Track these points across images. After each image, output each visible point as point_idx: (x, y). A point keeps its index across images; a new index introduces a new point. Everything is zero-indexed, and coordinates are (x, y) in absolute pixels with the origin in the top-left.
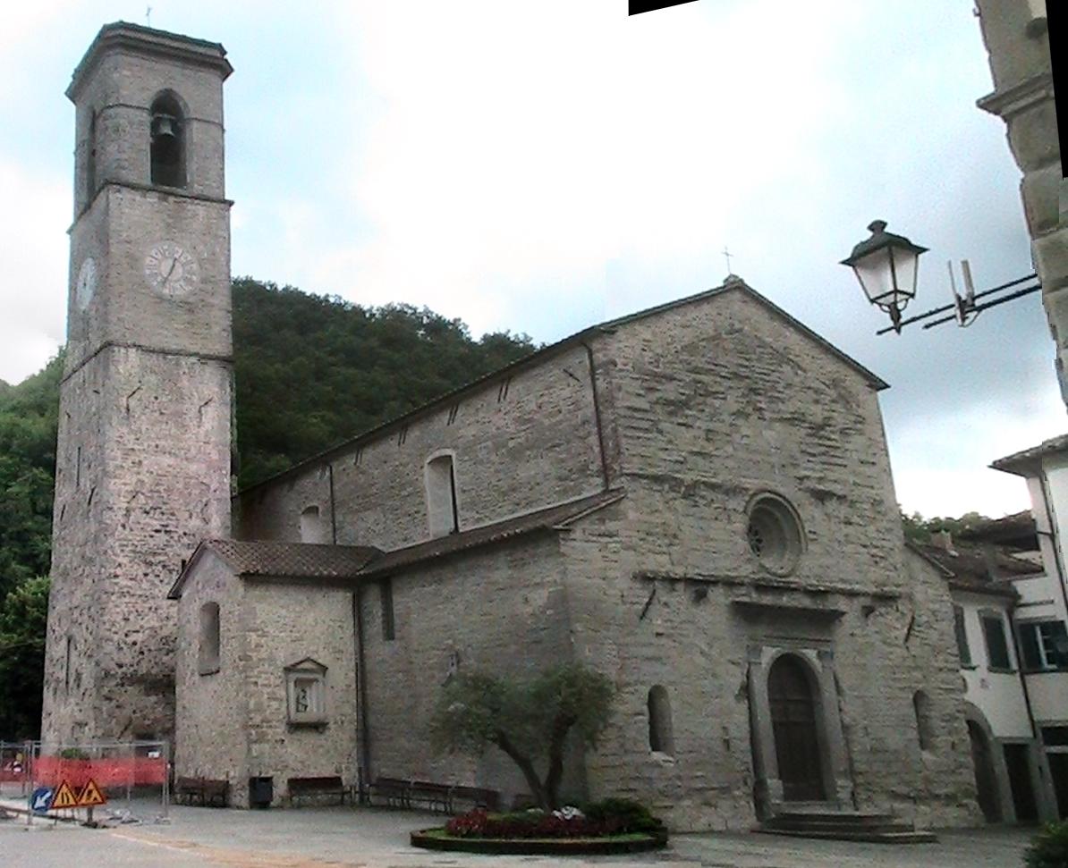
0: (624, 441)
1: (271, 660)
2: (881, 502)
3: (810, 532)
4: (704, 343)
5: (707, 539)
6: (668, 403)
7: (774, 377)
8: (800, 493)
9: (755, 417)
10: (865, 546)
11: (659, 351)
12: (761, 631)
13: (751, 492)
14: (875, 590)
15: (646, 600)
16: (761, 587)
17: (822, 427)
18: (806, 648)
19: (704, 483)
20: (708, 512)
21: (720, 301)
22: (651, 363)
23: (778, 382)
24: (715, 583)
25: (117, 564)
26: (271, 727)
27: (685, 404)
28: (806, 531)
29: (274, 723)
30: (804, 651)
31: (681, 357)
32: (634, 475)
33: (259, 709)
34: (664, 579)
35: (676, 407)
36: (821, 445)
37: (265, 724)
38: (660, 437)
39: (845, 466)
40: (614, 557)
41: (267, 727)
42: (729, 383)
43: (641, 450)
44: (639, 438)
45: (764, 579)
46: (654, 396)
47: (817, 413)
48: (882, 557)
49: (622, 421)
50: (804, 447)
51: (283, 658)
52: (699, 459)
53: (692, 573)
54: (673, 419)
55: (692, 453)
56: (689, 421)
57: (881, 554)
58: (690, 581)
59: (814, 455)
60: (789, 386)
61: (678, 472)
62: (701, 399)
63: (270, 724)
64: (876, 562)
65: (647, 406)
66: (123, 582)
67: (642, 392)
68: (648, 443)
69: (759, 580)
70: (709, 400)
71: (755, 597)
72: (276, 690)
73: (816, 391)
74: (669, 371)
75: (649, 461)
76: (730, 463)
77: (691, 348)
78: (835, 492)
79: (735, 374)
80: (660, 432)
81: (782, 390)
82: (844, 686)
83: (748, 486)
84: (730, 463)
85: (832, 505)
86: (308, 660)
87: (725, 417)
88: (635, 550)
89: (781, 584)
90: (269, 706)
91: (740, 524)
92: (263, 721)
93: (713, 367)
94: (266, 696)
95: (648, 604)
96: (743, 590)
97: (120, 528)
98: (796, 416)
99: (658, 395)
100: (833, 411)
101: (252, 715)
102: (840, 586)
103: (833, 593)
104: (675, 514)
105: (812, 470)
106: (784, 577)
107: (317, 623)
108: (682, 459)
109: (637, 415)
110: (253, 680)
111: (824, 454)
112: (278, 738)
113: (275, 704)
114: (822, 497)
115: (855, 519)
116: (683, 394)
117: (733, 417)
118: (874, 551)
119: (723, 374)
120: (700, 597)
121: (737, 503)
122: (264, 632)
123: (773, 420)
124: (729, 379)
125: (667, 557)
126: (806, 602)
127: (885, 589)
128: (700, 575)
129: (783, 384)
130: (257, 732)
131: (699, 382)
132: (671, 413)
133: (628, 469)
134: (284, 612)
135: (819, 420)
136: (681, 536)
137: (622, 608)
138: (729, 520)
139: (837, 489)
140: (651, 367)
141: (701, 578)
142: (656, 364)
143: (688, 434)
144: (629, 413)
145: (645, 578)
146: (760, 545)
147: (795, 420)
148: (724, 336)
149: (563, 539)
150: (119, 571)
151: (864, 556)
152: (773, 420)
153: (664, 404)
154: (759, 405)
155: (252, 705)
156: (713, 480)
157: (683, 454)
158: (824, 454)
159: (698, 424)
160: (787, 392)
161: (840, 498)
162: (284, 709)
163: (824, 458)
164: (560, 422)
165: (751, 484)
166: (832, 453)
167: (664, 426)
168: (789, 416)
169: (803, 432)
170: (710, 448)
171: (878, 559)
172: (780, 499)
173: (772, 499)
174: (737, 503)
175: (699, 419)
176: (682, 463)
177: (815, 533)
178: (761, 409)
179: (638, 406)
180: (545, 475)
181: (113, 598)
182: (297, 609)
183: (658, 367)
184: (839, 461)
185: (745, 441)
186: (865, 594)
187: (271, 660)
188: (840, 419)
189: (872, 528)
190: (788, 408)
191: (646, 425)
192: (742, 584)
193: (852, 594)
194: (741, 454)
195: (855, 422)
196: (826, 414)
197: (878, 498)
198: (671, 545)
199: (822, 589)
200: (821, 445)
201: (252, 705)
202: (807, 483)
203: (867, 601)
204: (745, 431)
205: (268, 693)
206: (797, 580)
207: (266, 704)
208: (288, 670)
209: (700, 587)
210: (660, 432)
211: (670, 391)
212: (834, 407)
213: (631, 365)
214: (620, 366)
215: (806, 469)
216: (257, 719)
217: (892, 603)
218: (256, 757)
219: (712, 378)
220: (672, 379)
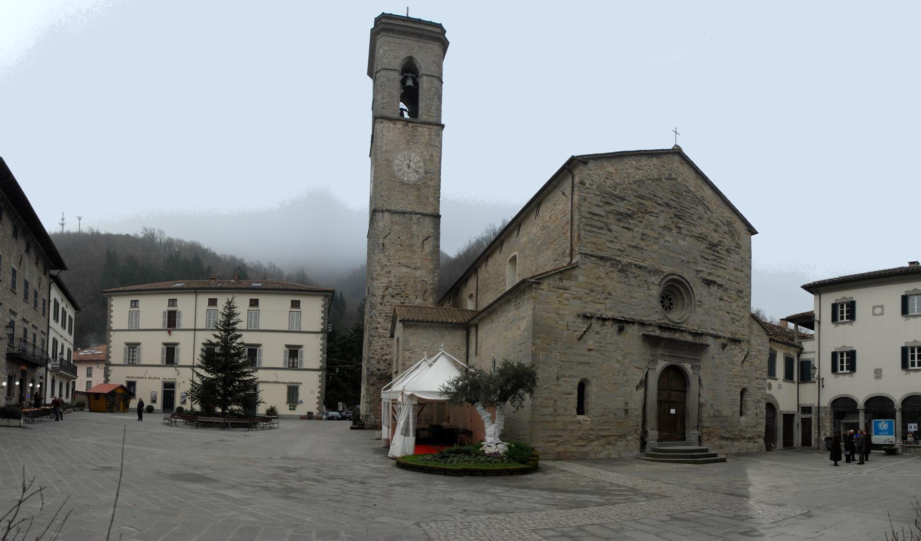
0: (583, 232)
2: (741, 292)
3: (698, 301)
4: (649, 182)
5: (631, 297)
6: (619, 214)
7: (692, 211)
8: (696, 279)
9: (675, 231)
10: (729, 313)
11: (618, 181)
12: (660, 352)
13: (665, 274)
14: (730, 336)
15: (585, 329)
16: (661, 328)
17: (716, 246)
18: (684, 362)
19: (636, 265)
20: (633, 282)
21: (664, 158)
22: (611, 187)
23: (694, 215)
24: (633, 322)
27: (630, 216)
28: (696, 299)
30: (683, 364)
31: (632, 187)
32: (586, 254)
34: (598, 318)
35: (622, 217)
36: (712, 255)
38: (609, 233)
39: (726, 269)
40: (566, 302)
42: (662, 209)
43: (594, 240)
44: (594, 232)
45: (664, 323)
46: (609, 208)
47: (715, 237)
48: (737, 320)
49: (584, 220)
50: (702, 254)
52: (634, 251)
53: (618, 316)
54: (622, 224)
55: (630, 246)
56: (631, 226)
57: (737, 318)
58: (615, 320)
59: (708, 260)
60: (701, 218)
61: (619, 256)
62: (640, 215)
64: (734, 322)
65: (603, 214)
67: (601, 204)
68: (599, 236)
69: (662, 324)
70: (647, 216)
71: (658, 333)
73: (717, 225)
74: (622, 195)
75: (599, 247)
76: (654, 256)
77: (640, 182)
78: (717, 282)
79: (667, 204)
81: (696, 219)
82: (703, 383)
83: (665, 270)
84: (654, 256)
85: (714, 288)
87: (656, 228)
88: (581, 300)
89: (675, 327)
91: (656, 291)
93: (652, 197)
95: (585, 332)
96: (651, 329)
98: (702, 236)
99: (613, 208)
100: (724, 238)
102: (711, 332)
103: (706, 335)
104: (613, 281)
105: (705, 268)
106: (678, 323)
108: (622, 249)
111: (714, 260)
114: (709, 283)
115: (725, 298)
116: (630, 210)
117: (661, 229)
118: (733, 316)
119: (658, 202)
120: (621, 330)
121: (655, 279)
123: (687, 235)
124: (663, 206)
125: (603, 306)
126: (689, 338)
127: (736, 336)
128: (624, 318)
129: (696, 216)
131: (642, 204)
132: (619, 220)
133: (584, 250)
135: (716, 241)
136: (614, 294)
137: (565, 333)
138: (649, 289)
139: (718, 280)
140: (609, 190)
141: (623, 319)
142: (613, 188)
143: (628, 234)
144: (590, 216)
145: (586, 317)
147: (700, 238)
148: (664, 180)
149: (535, 288)
151: (727, 318)
152: (687, 235)
154: (679, 225)
156: (642, 264)
157: (624, 246)
158: (714, 260)
159: (637, 229)
160: (699, 221)
161: (719, 285)
163: (714, 263)
165: (667, 269)
166: (719, 261)
167: (613, 227)
168: (697, 235)
169: (705, 246)
170: (642, 244)
171: (735, 321)
172: (684, 281)
173: (678, 280)
175: (637, 226)
176: (622, 251)
177: (701, 302)
178: (680, 228)
179: (596, 212)
183: (615, 190)
184: (722, 265)
185: (667, 244)
186: (725, 338)
188: (728, 242)
189: (734, 305)
190: (697, 231)
191: (601, 225)
192: (651, 325)
193: (716, 337)
194: (662, 251)
195: (736, 247)
196: (720, 239)
197: (741, 289)
198: (606, 298)
199: (699, 332)
200: (712, 255)
203: (725, 341)
204: (668, 238)
206: (686, 326)
209: (621, 324)
211: (622, 207)
212: (725, 236)
213: (595, 186)
215: (702, 266)
217: (738, 344)
219: (651, 203)
220: (623, 199)
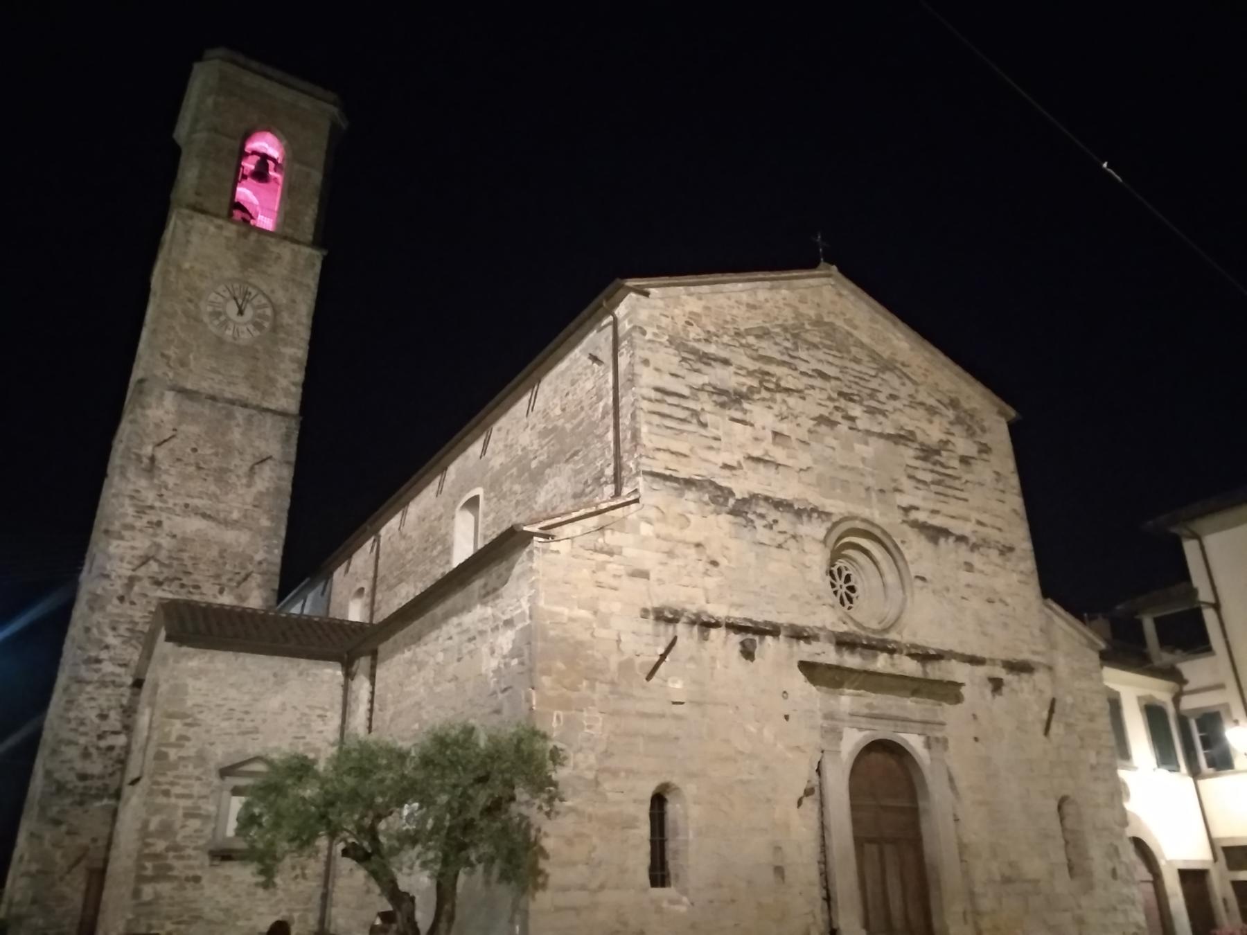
1: (201, 758)
13: (835, 519)
25: (103, 645)
26: (181, 858)
29: (189, 851)
33: (166, 830)
37: (171, 854)
41: (175, 857)
51: (220, 754)
63: (182, 853)
66: (108, 667)
72: (201, 802)
80: (704, 425)
85: (946, 544)
86: (257, 759)
90: (183, 827)
92: (168, 849)
94: (180, 812)
97: (116, 602)
101: (150, 840)
107: (284, 710)
109: (670, 400)
110: (165, 787)
112: (191, 873)
113: (195, 824)
122: (195, 719)
130: (155, 867)
132: (723, 405)
134: (232, 693)
146: (852, 595)
150: (104, 655)
153: (713, 393)
155: (153, 826)
162: (208, 830)
164: (580, 424)
174: (816, 529)
180: (562, 495)
181: (89, 688)
182: (255, 690)
187: (201, 758)
201: (153, 826)
202: (914, 515)
205: (184, 808)
207: (177, 825)
208: (225, 772)
210: (704, 425)
214: (649, 336)
216: (160, 845)
218: (149, 903)
